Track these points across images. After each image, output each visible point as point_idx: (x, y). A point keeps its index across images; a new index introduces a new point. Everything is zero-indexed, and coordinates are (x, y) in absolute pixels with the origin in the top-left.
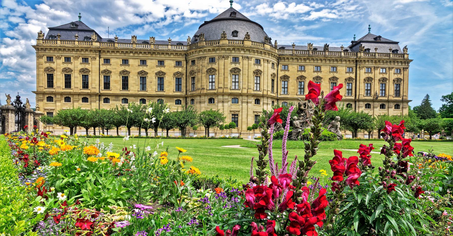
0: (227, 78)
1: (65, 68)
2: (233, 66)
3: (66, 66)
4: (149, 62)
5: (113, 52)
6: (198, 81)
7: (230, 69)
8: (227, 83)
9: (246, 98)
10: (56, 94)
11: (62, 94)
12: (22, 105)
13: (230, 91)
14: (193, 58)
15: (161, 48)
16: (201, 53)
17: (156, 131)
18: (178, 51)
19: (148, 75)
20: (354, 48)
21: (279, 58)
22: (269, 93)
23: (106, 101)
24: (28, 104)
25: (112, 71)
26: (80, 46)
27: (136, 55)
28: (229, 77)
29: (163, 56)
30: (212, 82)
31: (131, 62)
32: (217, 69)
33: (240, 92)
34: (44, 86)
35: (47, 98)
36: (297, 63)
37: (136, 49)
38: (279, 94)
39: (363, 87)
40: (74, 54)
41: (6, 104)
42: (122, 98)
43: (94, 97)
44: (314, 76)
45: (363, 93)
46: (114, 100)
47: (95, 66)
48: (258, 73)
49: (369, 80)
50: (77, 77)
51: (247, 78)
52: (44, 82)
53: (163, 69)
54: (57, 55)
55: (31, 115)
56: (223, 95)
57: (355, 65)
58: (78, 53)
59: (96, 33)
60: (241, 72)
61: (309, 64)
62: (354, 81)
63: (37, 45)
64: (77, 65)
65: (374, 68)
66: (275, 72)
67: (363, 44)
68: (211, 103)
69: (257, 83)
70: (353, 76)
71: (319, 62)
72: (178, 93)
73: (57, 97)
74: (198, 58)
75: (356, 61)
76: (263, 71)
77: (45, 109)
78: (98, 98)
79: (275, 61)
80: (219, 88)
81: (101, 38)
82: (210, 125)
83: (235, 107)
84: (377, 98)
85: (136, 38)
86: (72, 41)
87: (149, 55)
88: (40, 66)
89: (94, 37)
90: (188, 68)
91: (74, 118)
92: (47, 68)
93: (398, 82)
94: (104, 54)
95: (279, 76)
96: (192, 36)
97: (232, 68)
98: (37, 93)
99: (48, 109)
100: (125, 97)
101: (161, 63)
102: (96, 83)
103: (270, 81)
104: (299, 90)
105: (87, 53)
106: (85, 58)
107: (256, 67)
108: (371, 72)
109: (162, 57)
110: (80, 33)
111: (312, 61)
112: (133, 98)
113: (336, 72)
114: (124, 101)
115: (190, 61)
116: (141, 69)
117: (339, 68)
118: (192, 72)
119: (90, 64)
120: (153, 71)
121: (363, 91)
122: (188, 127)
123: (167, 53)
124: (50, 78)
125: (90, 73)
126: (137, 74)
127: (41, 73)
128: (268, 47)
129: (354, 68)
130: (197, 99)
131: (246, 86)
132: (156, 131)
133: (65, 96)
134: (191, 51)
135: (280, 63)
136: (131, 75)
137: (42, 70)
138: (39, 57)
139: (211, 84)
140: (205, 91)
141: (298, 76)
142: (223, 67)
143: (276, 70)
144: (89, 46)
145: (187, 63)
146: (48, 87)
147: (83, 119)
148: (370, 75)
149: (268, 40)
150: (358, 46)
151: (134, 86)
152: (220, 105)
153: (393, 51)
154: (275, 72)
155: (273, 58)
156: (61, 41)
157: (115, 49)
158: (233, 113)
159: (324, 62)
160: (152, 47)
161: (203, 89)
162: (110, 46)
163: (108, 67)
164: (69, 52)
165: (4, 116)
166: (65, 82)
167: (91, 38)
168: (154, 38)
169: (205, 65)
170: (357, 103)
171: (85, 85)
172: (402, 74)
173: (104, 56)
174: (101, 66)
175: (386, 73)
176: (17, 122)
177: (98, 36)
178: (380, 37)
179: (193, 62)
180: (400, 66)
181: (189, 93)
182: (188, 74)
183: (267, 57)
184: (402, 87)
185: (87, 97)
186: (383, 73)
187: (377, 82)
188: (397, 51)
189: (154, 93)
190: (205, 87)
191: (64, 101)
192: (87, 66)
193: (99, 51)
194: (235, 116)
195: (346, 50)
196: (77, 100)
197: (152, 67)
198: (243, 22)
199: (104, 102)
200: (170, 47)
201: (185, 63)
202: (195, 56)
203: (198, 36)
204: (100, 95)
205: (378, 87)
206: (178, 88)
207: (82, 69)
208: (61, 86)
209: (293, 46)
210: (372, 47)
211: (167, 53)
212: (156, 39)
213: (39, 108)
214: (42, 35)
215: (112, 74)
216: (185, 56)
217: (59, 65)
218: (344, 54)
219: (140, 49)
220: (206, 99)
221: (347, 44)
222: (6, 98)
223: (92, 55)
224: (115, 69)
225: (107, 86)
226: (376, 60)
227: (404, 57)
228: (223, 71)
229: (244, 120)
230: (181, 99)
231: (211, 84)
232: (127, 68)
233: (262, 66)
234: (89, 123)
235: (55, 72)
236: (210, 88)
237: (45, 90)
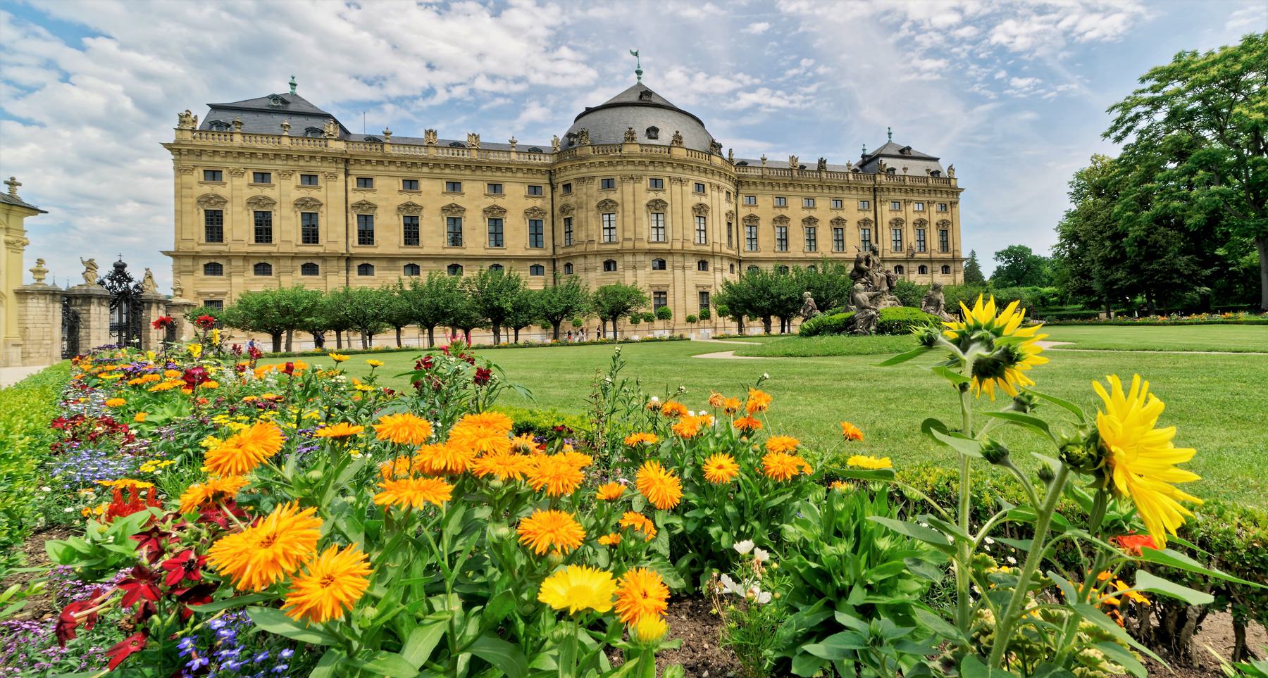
1: (255, 198)
3: (257, 191)
4: (466, 187)
5: (380, 162)
6: (580, 226)
8: (645, 228)
9: (681, 259)
10: (229, 257)
11: (246, 257)
12: (132, 285)
13: (647, 246)
15: (493, 157)
16: (584, 170)
17: (497, 333)
19: (467, 214)
20: (867, 167)
21: (738, 183)
22: (725, 249)
23: (365, 269)
24: (148, 282)
26: (295, 147)
28: (645, 218)
29: (499, 174)
30: (610, 228)
31: (424, 185)
33: (668, 247)
34: (196, 238)
35: (206, 266)
37: (436, 159)
40: (279, 164)
41: (83, 282)
42: (406, 263)
43: (335, 263)
46: (384, 269)
47: (334, 194)
48: (701, 211)
49: (897, 224)
50: (289, 218)
52: (196, 229)
53: (499, 202)
54: (232, 166)
55: (158, 308)
56: (634, 254)
59: (336, 122)
60: (669, 209)
63: (176, 143)
66: (732, 208)
68: (609, 269)
69: (700, 230)
70: (871, 216)
71: (812, 190)
72: (536, 252)
73: (234, 263)
74: (578, 180)
75: (875, 190)
77: (200, 294)
78: (343, 264)
79: (732, 189)
81: (347, 133)
82: (618, 313)
83: (660, 278)
85: (435, 134)
86: (273, 136)
87: (468, 172)
88: (185, 192)
90: (557, 199)
91: (286, 311)
92: (206, 196)
93: (945, 231)
94: (357, 166)
96: (561, 135)
98: (176, 256)
99: (207, 294)
101: (496, 188)
102: (336, 232)
103: (725, 226)
104: (778, 243)
105: (313, 163)
106: (310, 176)
107: (698, 199)
108: (900, 210)
109: (497, 177)
110: (295, 119)
111: (799, 189)
112: (431, 264)
113: (842, 208)
114: (409, 271)
115: (560, 186)
116: (449, 200)
117: (846, 203)
118: (565, 209)
119: (323, 190)
120: (478, 206)
122: (566, 325)
123: (509, 168)
125: (323, 209)
126: (439, 212)
127: (187, 208)
128: (716, 160)
130: (578, 264)
132: (497, 333)
133: (256, 262)
134: (562, 166)
136: (424, 212)
137: (191, 200)
138: (180, 170)
139: (607, 232)
140: (596, 247)
144: (318, 148)
145: (553, 189)
146: (208, 240)
147: (309, 311)
148: (900, 215)
149: (715, 147)
150: (874, 163)
151: (433, 237)
152: (629, 273)
153: (932, 173)
154: (732, 208)
156: (243, 135)
157: (385, 157)
158: (656, 289)
159: (819, 190)
160: (474, 155)
161: (592, 242)
162: (374, 151)
163: (369, 196)
164: (266, 161)
165: (74, 312)
166: (256, 230)
167: (322, 132)
168: (477, 137)
169: (594, 192)
171: (311, 235)
173: (357, 171)
174: (350, 194)
175: (923, 211)
176: (116, 328)
177: (342, 127)
178: (909, 148)
179: (567, 187)
180: (945, 199)
182: (556, 211)
183: (716, 180)
185: (315, 262)
186: (918, 211)
188: (938, 172)
189: (481, 251)
190: (595, 238)
191: (252, 272)
192: (314, 194)
193: (346, 161)
194: (661, 295)
195: (855, 171)
196: (290, 269)
197: (474, 197)
199: (360, 274)
200: (514, 156)
201: (548, 189)
202: (570, 175)
203: (576, 136)
204: (349, 259)
207: (301, 199)
208: (246, 239)
209: (764, 159)
210: (898, 164)
211: (509, 168)
212: (482, 140)
213: (181, 290)
215: (378, 211)
216: (547, 176)
217: (237, 192)
219: (446, 159)
220: (599, 262)
221: (856, 159)
222: (84, 269)
223: (329, 168)
224: (387, 199)
225: (366, 236)
226: (908, 188)
229: (680, 303)
230: (542, 264)
231: (607, 232)
232: (415, 199)
234: (323, 321)
236: (607, 239)
237: (199, 249)
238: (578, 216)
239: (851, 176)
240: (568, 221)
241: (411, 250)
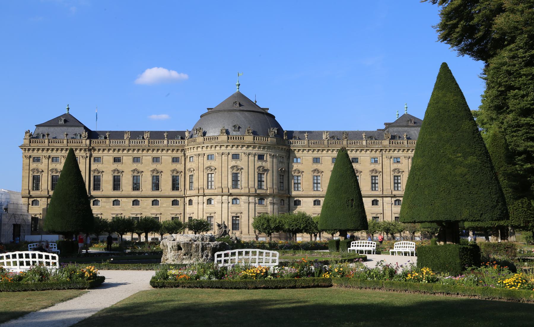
7: (229, 167)
14: (191, 154)
36: (310, 155)
46: (105, 202)
53: (159, 167)
57: (381, 155)
62: (381, 173)
67: (391, 129)
80: (218, 187)
89: (85, 134)
97: (232, 165)
120: (148, 170)
129: (381, 158)
143: (286, 165)
145: (185, 159)
173: (95, 154)
198: (246, 113)
201: (183, 158)
218: (366, 144)
220: (206, 198)
223: (83, 153)
230: (178, 199)
235: (43, 173)
238: (196, 174)
239: (364, 143)
241: (117, 193)
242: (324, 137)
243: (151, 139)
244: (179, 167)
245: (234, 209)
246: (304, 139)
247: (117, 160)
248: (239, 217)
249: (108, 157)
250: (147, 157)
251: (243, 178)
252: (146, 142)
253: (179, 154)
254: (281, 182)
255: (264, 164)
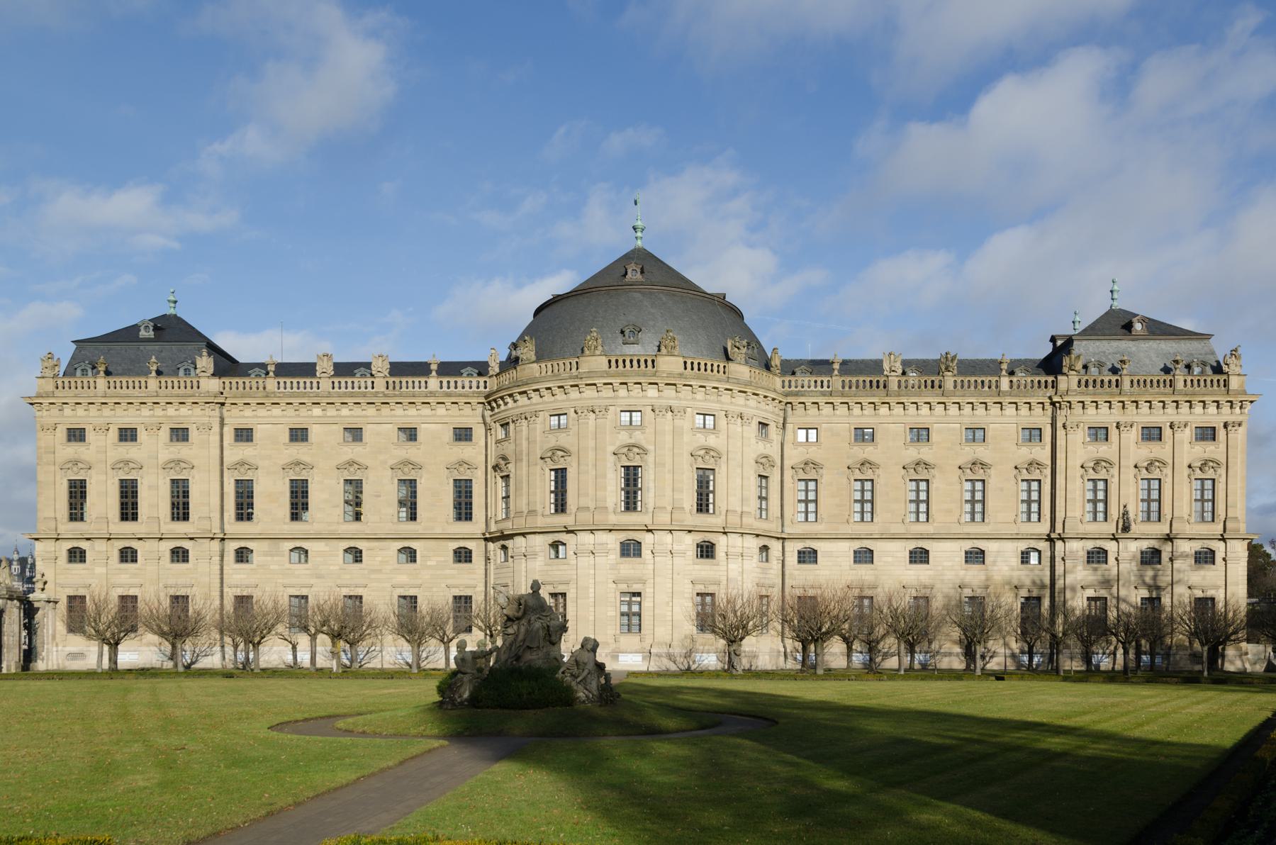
0: (604, 476)
2: (624, 438)
7: (611, 449)
18: (460, 395)
25: (260, 463)
27: (331, 411)
31: (315, 432)
32: (573, 449)
38: (787, 522)
39: (1078, 493)
42: (292, 545)
44: (907, 461)
45: (1078, 514)
51: (668, 476)
58: (158, 411)
61: (890, 420)
62: (1048, 471)
64: (153, 450)
65: (1118, 427)
70: (1043, 454)
76: (723, 450)
84: (1126, 529)
89: (205, 362)
94: (235, 410)
95: (787, 463)
97: (618, 444)
100: (298, 544)
103: (753, 482)
114: (295, 555)
121: (1079, 504)
124: (78, 492)
131: (667, 502)
135: (789, 420)
141: (850, 462)
142: (591, 443)
145: (488, 429)
155: (763, 405)
170: (1059, 544)
171: (181, 510)
172: (1223, 447)
173: (237, 417)
181: (493, 528)
184: (1220, 487)
187: (1129, 473)
190: (539, 508)
205: (1132, 490)
206: (463, 510)
214: (51, 363)
227: (1226, 384)
228: (591, 455)
230: (470, 545)
233: (723, 436)
235: (92, 472)
240: (506, 478)
241: (297, 527)
242: (886, 366)
243: (392, 374)
244: (473, 452)
245: (629, 567)
246: (830, 372)
247: (299, 435)
248: (639, 594)
249: (269, 423)
250: (381, 426)
251: (648, 480)
252: (380, 384)
253: (471, 417)
254: (760, 498)
255: (712, 441)
